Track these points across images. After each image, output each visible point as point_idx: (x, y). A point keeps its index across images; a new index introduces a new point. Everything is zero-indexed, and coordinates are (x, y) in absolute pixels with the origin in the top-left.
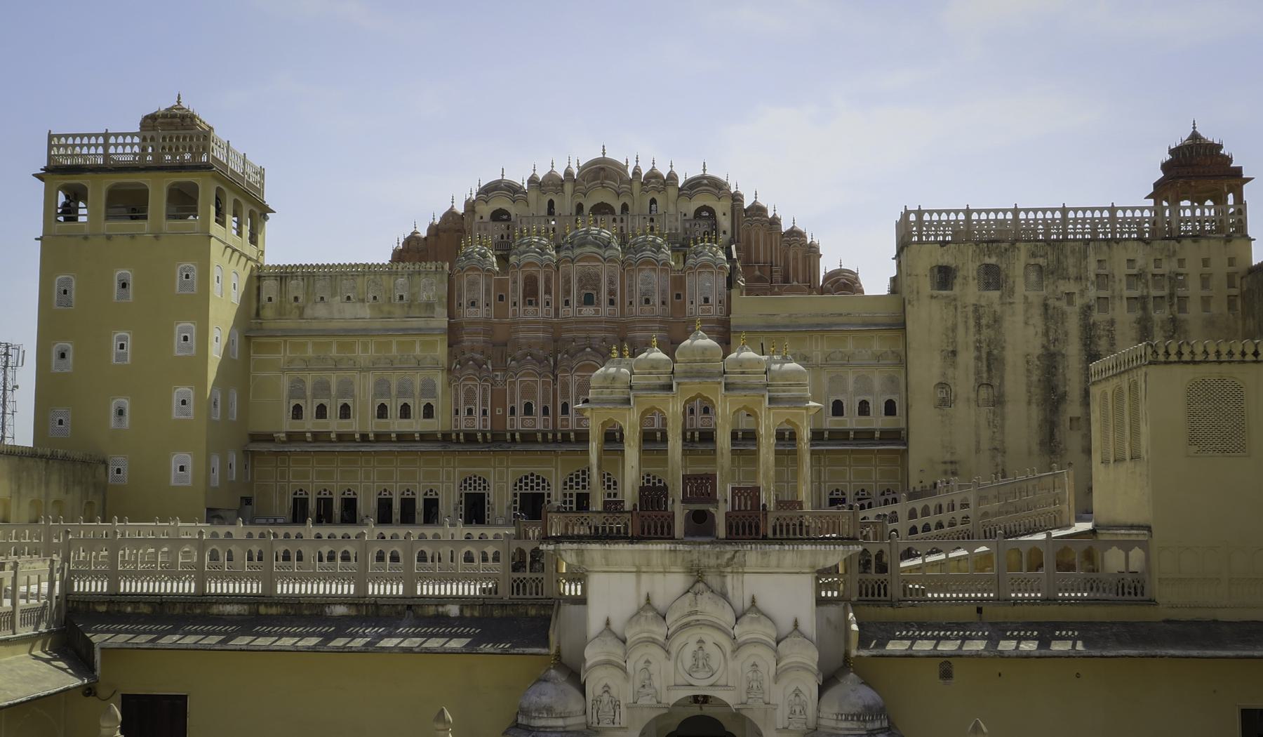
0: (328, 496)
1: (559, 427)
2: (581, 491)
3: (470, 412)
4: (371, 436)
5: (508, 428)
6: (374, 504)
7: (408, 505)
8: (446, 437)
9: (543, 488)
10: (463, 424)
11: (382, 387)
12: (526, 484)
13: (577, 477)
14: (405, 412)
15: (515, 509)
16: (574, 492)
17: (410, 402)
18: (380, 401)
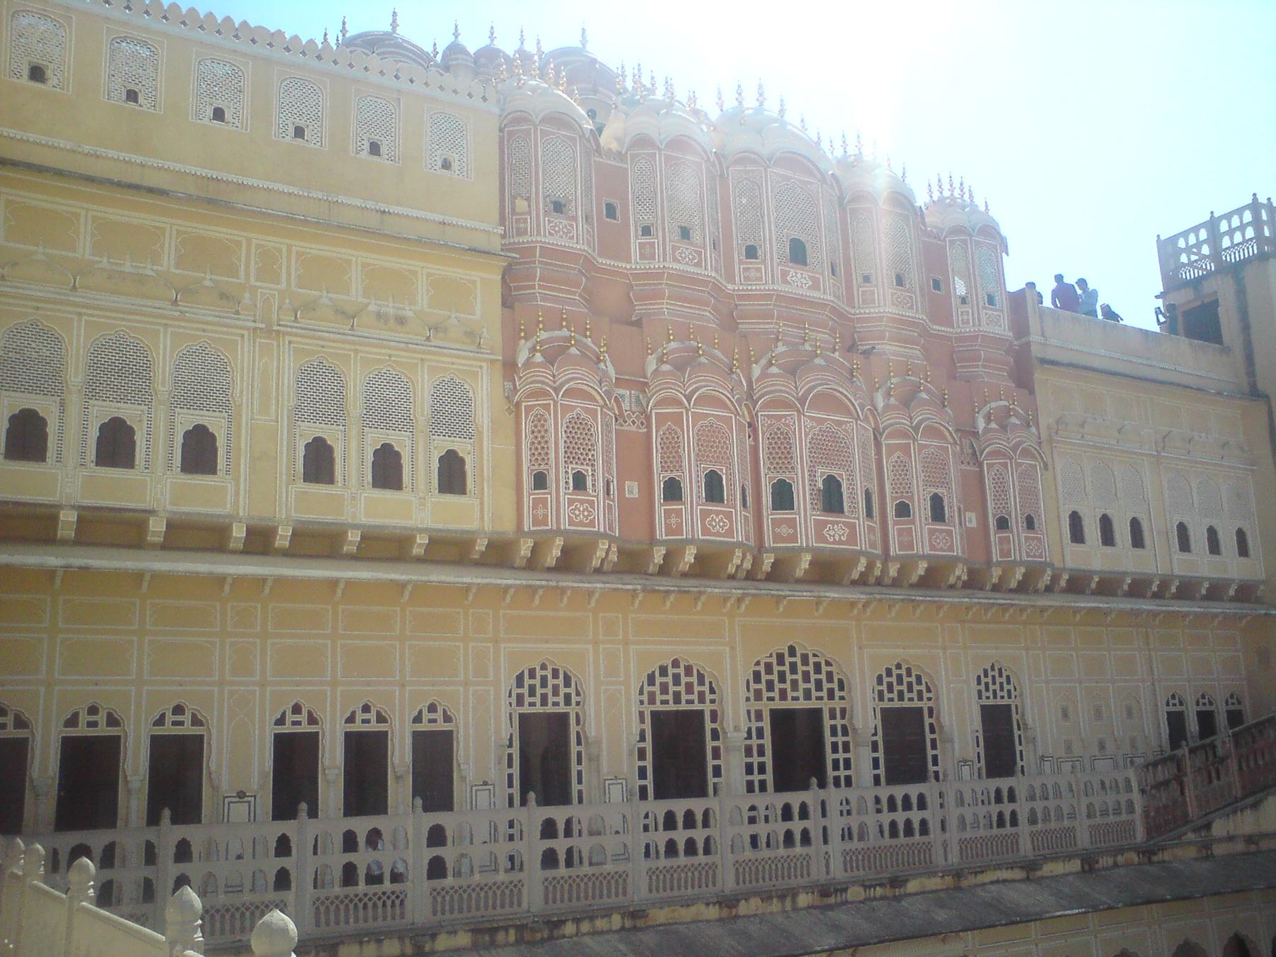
0: (103, 730)
1: (769, 542)
2: (779, 705)
3: (579, 482)
4: (283, 538)
5: (661, 533)
6: (263, 761)
7: (366, 753)
8: (498, 554)
9: (702, 699)
10: (565, 512)
11: (320, 390)
12: (664, 688)
13: (769, 668)
14: (387, 469)
15: (642, 754)
16: (766, 707)
17: (400, 441)
18: (310, 430)
